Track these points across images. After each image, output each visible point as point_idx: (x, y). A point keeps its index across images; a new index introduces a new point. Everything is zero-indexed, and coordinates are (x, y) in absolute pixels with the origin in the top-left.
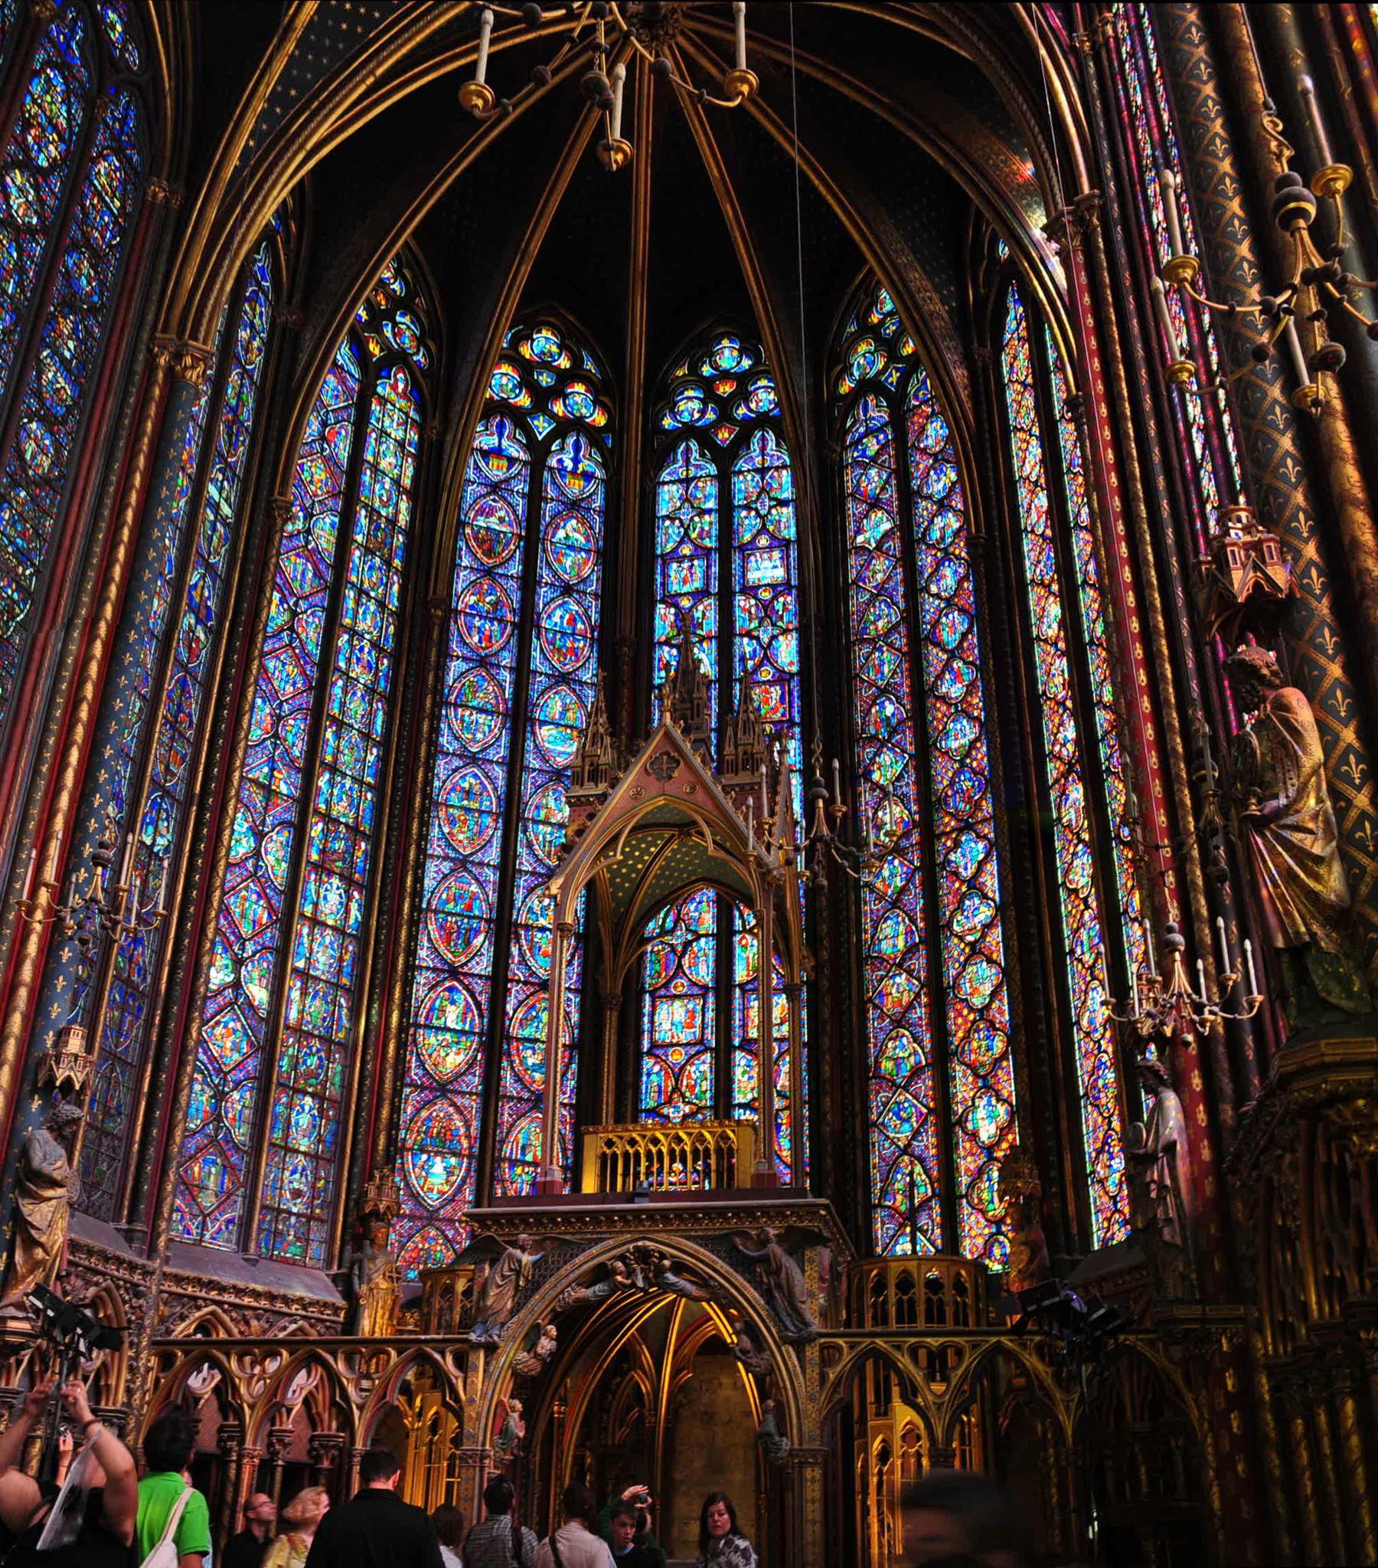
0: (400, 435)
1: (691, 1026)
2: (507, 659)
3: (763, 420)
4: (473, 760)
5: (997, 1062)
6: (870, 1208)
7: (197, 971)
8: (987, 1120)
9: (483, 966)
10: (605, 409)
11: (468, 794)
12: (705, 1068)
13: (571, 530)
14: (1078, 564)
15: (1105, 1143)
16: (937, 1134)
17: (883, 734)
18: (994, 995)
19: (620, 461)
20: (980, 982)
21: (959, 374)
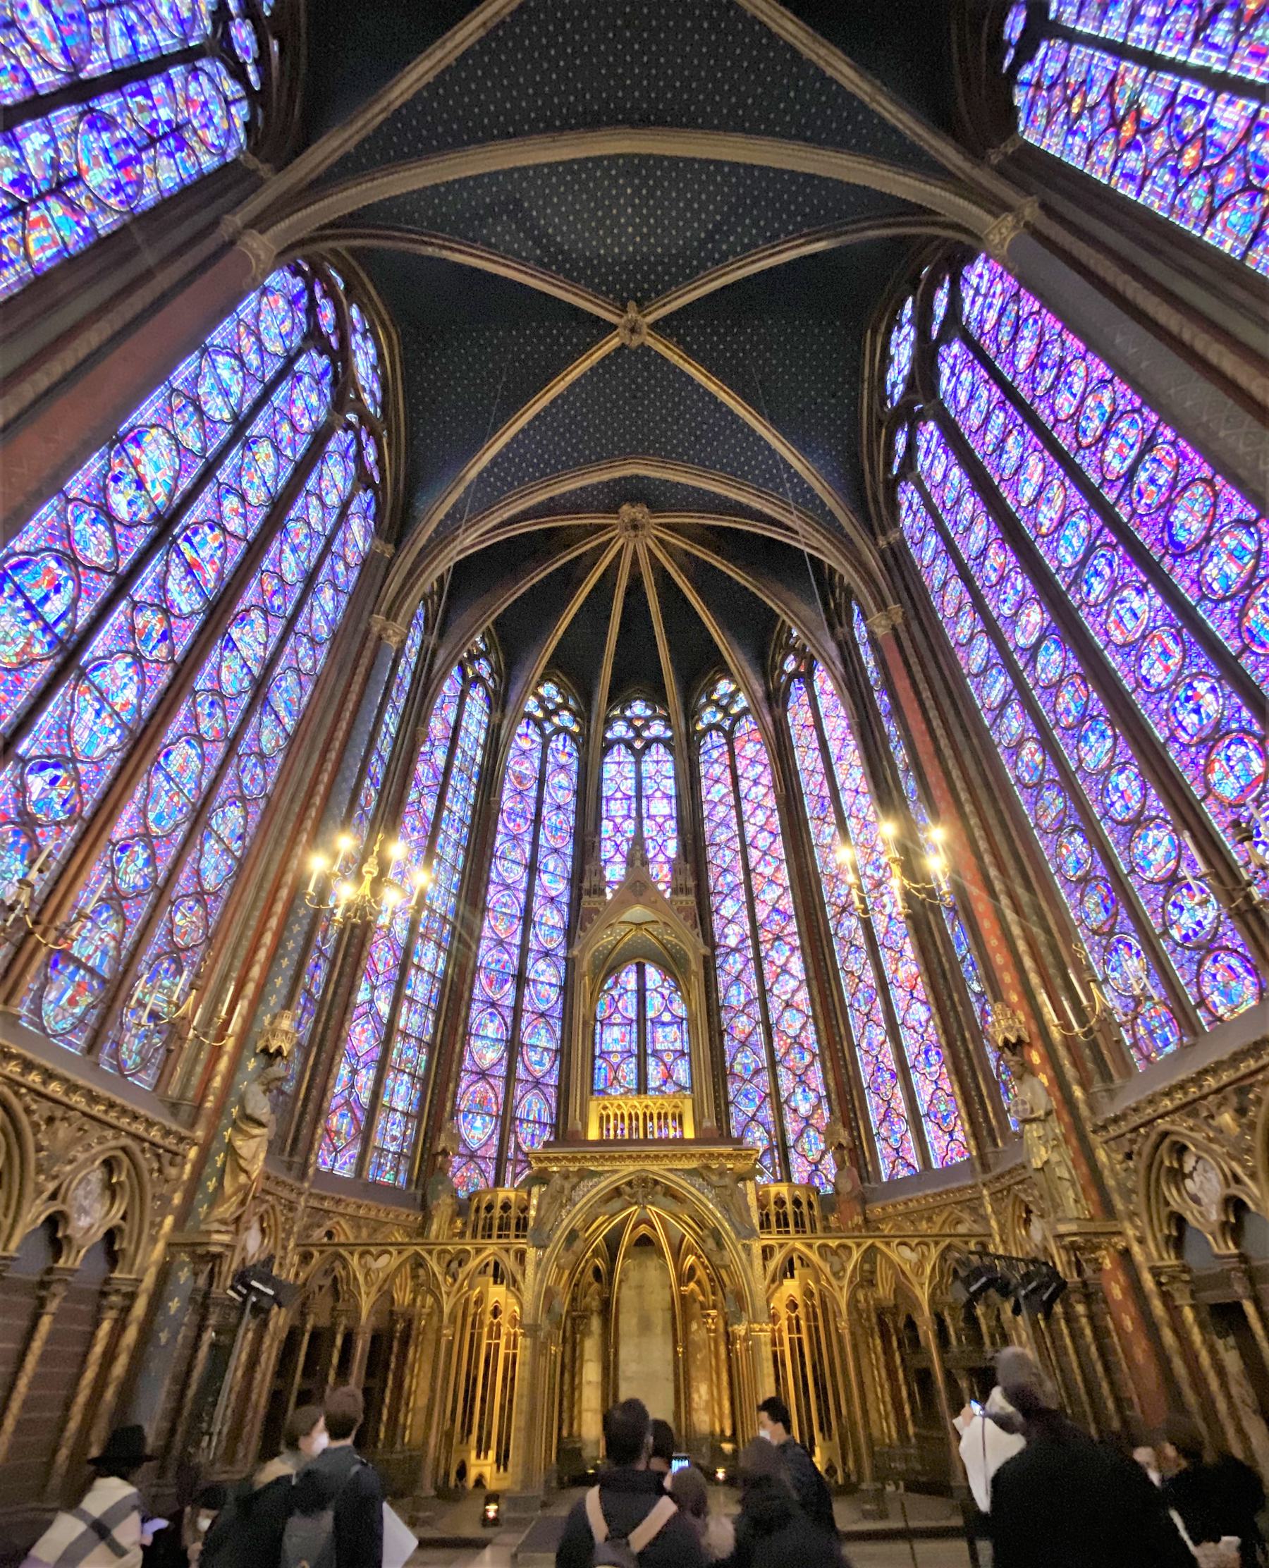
2: (528, 838)
4: (508, 887)
5: (808, 1067)
7: (352, 989)
9: (510, 1001)
11: (505, 905)
12: (633, 1066)
13: (562, 779)
15: (886, 1115)
17: (726, 891)
18: (803, 1027)
20: (792, 1023)
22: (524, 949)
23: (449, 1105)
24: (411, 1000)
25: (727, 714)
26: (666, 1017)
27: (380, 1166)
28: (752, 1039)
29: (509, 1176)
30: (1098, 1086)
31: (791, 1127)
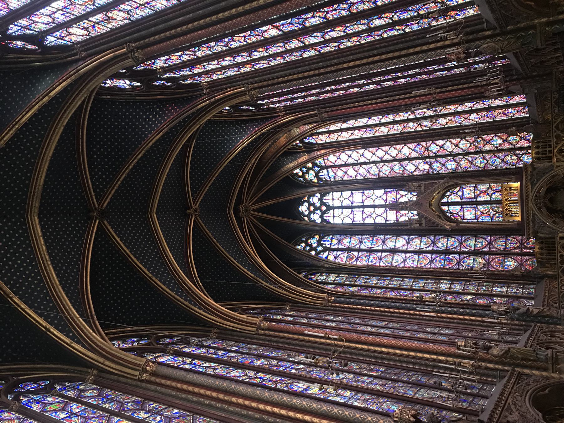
0: (325, 277)
1: (471, 210)
3: (321, 199)
5: (483, 140)
6: (516, 168)
8: (497, 142)
10: (315, 235)
11: (414, 261)
12: (481, 207)
14: (375, 123)
15: (505, 114)
16: (499, 153)
17: (402, 169)
18: (468, 141)
19: (329, 231)
20: (464, 145)
21: (323, 151)
22: (432, 252)
23: (503, 273)
24: (464, 289)
25: (312, 169)
26: (460, 193)
27: (528, 293)
28: (470, 159)
29: (528, 251)
30: (514, 72)
31: (507, 146)
